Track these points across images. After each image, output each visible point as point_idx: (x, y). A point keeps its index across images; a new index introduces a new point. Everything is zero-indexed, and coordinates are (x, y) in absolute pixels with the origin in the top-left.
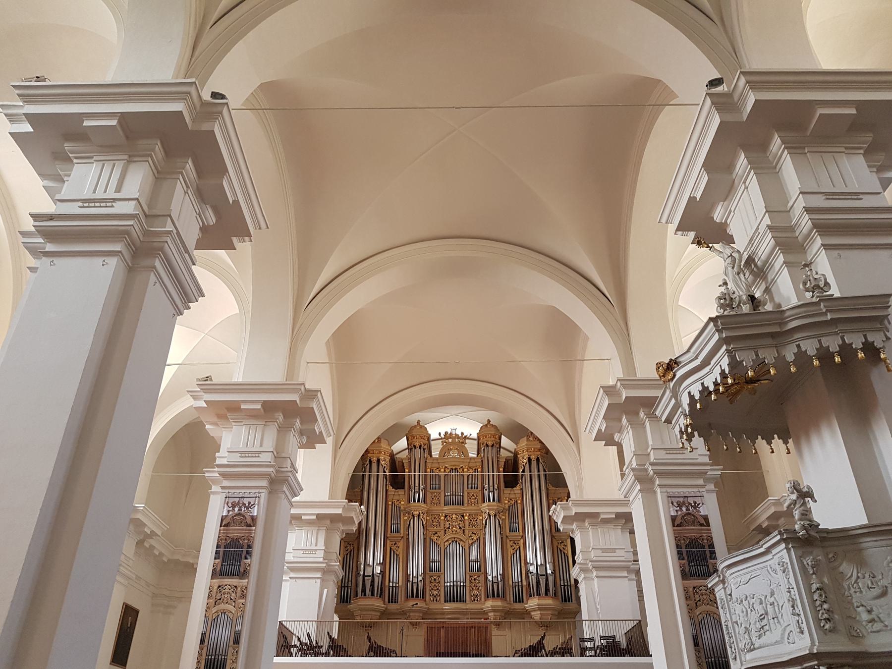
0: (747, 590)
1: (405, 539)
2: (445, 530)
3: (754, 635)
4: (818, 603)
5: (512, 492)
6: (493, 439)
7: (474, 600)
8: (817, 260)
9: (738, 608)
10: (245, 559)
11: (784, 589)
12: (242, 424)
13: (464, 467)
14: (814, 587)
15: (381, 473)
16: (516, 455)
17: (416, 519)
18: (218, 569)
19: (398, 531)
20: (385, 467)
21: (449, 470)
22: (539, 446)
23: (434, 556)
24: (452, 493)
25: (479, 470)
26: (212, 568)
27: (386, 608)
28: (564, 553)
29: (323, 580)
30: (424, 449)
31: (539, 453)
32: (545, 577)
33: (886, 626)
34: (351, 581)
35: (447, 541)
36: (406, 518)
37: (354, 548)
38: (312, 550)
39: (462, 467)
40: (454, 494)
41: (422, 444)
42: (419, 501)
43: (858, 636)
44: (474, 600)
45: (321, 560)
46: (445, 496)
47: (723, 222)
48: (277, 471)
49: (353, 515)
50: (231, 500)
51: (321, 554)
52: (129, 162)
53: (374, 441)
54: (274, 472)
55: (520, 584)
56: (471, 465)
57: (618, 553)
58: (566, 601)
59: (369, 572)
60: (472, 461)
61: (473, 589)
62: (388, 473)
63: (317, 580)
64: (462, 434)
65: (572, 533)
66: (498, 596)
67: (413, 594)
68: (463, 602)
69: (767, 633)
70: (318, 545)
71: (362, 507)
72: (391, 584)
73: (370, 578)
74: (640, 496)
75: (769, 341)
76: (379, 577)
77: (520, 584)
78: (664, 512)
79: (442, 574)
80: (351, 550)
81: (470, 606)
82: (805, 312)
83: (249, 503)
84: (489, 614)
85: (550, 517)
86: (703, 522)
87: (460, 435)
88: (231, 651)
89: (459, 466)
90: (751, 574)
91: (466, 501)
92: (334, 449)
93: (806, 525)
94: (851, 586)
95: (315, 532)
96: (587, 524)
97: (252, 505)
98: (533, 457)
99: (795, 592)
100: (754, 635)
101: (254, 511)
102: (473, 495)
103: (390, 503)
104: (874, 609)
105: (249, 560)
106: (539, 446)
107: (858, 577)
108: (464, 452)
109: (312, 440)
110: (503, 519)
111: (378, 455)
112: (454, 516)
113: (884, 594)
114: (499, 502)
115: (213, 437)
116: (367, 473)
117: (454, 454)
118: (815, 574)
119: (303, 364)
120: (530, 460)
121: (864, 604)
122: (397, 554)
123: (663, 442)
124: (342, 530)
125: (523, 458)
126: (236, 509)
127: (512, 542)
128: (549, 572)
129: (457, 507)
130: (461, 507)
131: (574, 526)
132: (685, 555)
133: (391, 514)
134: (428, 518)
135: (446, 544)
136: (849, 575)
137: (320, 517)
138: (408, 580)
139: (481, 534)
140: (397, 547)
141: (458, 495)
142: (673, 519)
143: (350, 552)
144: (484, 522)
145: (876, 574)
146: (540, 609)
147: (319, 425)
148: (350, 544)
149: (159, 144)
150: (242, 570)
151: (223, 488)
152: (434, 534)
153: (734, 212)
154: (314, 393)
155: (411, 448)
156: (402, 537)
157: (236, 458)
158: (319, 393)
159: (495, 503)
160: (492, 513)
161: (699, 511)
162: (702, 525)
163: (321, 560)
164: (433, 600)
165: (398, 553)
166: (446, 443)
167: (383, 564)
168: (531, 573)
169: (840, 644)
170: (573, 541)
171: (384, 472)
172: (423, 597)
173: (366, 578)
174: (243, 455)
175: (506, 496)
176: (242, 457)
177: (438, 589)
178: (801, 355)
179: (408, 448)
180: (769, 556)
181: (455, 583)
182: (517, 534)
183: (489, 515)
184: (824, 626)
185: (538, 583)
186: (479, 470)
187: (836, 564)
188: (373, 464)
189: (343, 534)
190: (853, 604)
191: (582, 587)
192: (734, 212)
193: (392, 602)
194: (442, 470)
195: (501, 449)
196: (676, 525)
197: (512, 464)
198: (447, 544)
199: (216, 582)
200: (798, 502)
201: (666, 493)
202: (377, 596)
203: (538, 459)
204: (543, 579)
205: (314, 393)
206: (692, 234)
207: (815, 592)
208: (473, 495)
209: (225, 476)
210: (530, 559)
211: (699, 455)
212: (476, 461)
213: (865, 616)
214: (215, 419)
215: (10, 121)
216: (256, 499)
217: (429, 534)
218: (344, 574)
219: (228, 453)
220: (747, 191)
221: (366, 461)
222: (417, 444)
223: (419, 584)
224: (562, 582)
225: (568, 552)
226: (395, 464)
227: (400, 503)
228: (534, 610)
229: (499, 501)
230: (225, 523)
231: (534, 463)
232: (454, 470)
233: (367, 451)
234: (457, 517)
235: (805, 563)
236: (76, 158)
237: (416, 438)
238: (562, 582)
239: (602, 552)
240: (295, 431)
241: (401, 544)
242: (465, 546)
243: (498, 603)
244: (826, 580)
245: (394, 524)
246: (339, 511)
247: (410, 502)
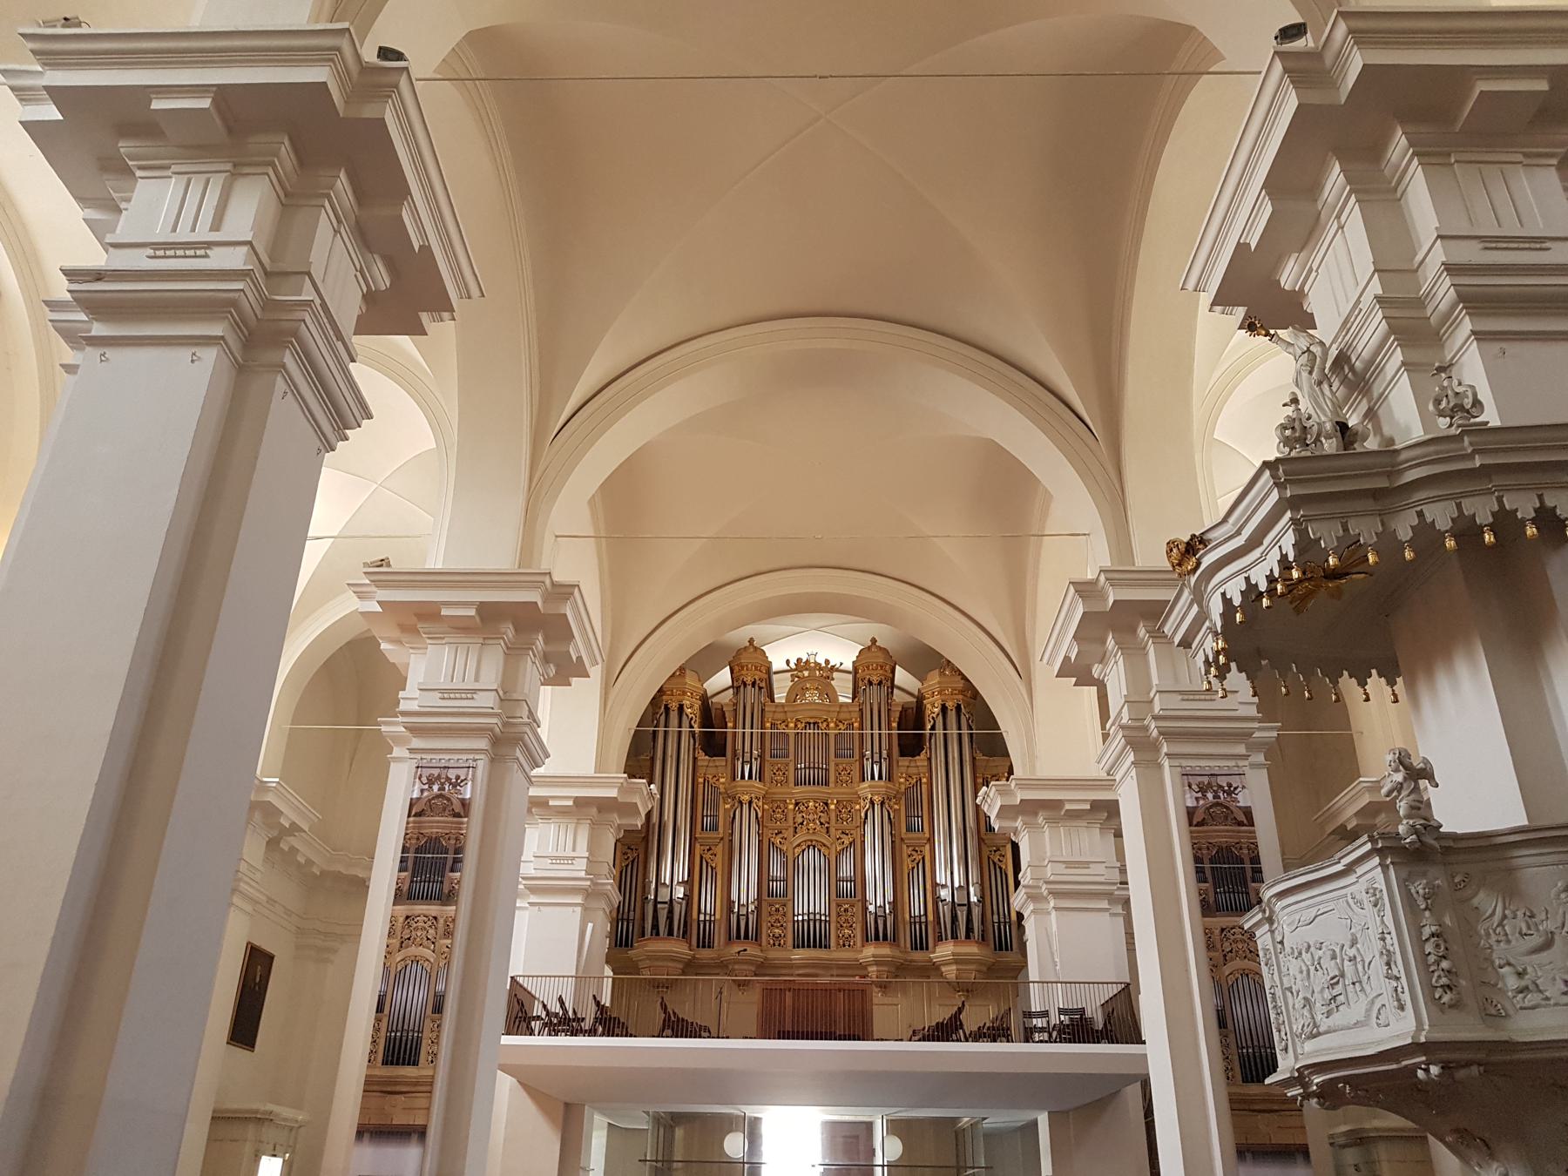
0: (1310, 935)
1: (726, 840)
2: (796, 828)
3: (1319, 1009)
4: (1432, 959)
5: (913, 764)
6: (881, 672)
7: (844, 945)
8: (1463, 358)
9: (1293, 966)
10: (452, 870)
11: (1374, 933)
12: (444, 642)
13: (829, 720)
14: (1427, 932)
15: (685, 729)
16: (920, 699)
17: (746, 807)
18: (405, 888)
19: (715, 828)
20: (692, 719)
21: (803, 725)
22: (961, 684)
23: (776, 871)
24: (807, 764)
25: (856, 725)
26: (394, 887)
27: (694, 957)
28: (1000, 868)
29: (585, 909)
30: (760, 688)
31: (961, 697)
32: (965, 908)
33: (1547, 999)
34: (634, 911)
35: (799, 845)
36: (727, 806)
37: (638, 856)
38: (567, 858)
39: (826, 720)
40: (812, 765)
41: (757, 679)
42: (750, 777)
43: (1499, 1016)
44: (844, 945)
45: (583, 874)
46: (796, 769)
47: (1297, 289)
48: (505, 724)
49: (637, 800)
50: (426, 772)
51: (582, 864)
52: (235, 175)
53: (674, 673)
55: (923, 919)
56: (842, 716)
57: (1094, 869)
58: (1001, 949)
59: (664, 895)
60: (845, 709)
61: (841, 926)
62: (697, 729)
64: (827, 662)
65: (1015, 834)
66: (885, 938)
67: (740, 934)
68: (825, 947)
69: (1341, 1008)
70: (578, 848)
71: (652, 786)
72: (702, 917)
73: (666, 906)
74: (1133, 773)
75: (1369, 504)
76: (681, 904)
77: (923, 919)
78: (1175, 800)
79: (789, 900)
80: (634, 859)
81: (835, 954)
82: (1437, 453)
83: (458, 777)
84: (870, 969)
85: (977, 807)
86: (1242, 818)
87: (824, 665)
88: (428, 1024)
89: (820, 718)
90: (1317, 908)
91: (832, 779)
92: (604, 686)
93: (1418, 826)
94: (1491, 931)
95: (571, 827)
96: (1040, 819)
97: (462, 781)
98: (950, 705)
99: (1392, 940)
100: (1319, 1009)
101: (465, 791)
102: (845, 769)
103: (701, 780)
104: (1529, 970)
105: (459, 874)
106: (961, 684)
107: (1504, 917)
108: (830, 694)
109: (564, 670)
110: (895, 810)
111: (681, 698)
112: (811, 804)
113: (1548, 944)
114: (889, 780)
115: (394, 664)
116: (662, 729)
117: (812, 697)
118: (1430, 910)
119: (549, 539)
120: (944, 709)
121: (1512, 961)
122: (712, 867)
123: (1176, 680)
124: (619, 825)
125: (933, 706)
126: (436, 787)
127: (910, 849)
128: (974, 899)
129: (816, 788)
130: (824, 789)
131: (1019, 823)
132: (1208, 874)
133: (702, 800)
134: (766, 806)
135: (796, 850)
136: (1490, 911)
137: (580, 803)
138: (730, 910)
139: (857, 834)
140: (712, 855)
141: (818, 768)
142: (1191, 813)
143: (633, 862)
144: (863, 815)
145: (1535, 911)
146: (956, 962)
147: (576, 646)
148: (632, 850)
149: (287, 142)
150: (446, 891)
151: (411, 750)
152: (776, 834)
153: (1317, 271)
154: (569, 590)
155: (738, 685)
156: (722, 839)
157: (434, 700)
158: (576, 590)
159: (882, 783)
160: (877, 799)
161: (1236, 800)
162: (1240, 824)
163: (583, 874)
164: (774, 945)
165: (714, 865)
166: (798, 677)
167: (688, 883)
168: (942, 901)
169: (1467, 1029)
170: (1015, 848)
171: (691, 727)
172: (757, 938)
173: (659, 906)
174: (446, 695)
175: (903, 769)
176: (444, 699)
177: (782, 926)
178: (1426, 534)
179: (732, 687)
180: (1351, 879)
181: (812, 917)
182: (920, 835)
183: (872, 803)
184: (1440, 997)
185: (954, 918)
186: (856, 725)
187: (1469, 892)
188: (671, 712)
189: (620, 831)
190: (1492, 962)
191: (1029, 924)
192: (1317, 271)
193: (704, 947)
194: (792, 725)
195: (895, 691)
196: (1195, 823)
197: (913, 716)
198: (798, 850)
199: (402, 910)
200: (1405, 785)
201: (1179, 769)
202: (678, 936)
203: (958, 708)
204: (962, 912)
205: (569, 590)
206: (1240, 312)
207: (1427, 940)
208: (845, 769)
209: (416, 730)
210: (941, 878)
211: (1241, 703)
212: (851, 709)
213: (1512, 983)
214: (396, 633)
215: (21, 100)
216: (468, 771)
217: (768, 833)
218: (622, 899)
219: (419, 691)
220: (1343, 232)
221: (659, 708)
222: (749, 680)
223: (750, 916)
224: (996, 917)
225: (1006, 867)
226: (709, 713)
227: (718, 780)
228: (947, 964)
229: (890, 779)
230: (416, 810)
231: (952, 715)
232: (812, 725)
233: (661, 691)
234: (817, 805)
235: (1413, 891)
236: (141, 168)
237: (747, 670)
238: (996, 917)
240: (535, 656)
241: (719, 849)
242: (829, 855)
243: (885, 950)
244: (1447, 921)
245: (707, 816)
246: (613, 793)
247: (734, 780)
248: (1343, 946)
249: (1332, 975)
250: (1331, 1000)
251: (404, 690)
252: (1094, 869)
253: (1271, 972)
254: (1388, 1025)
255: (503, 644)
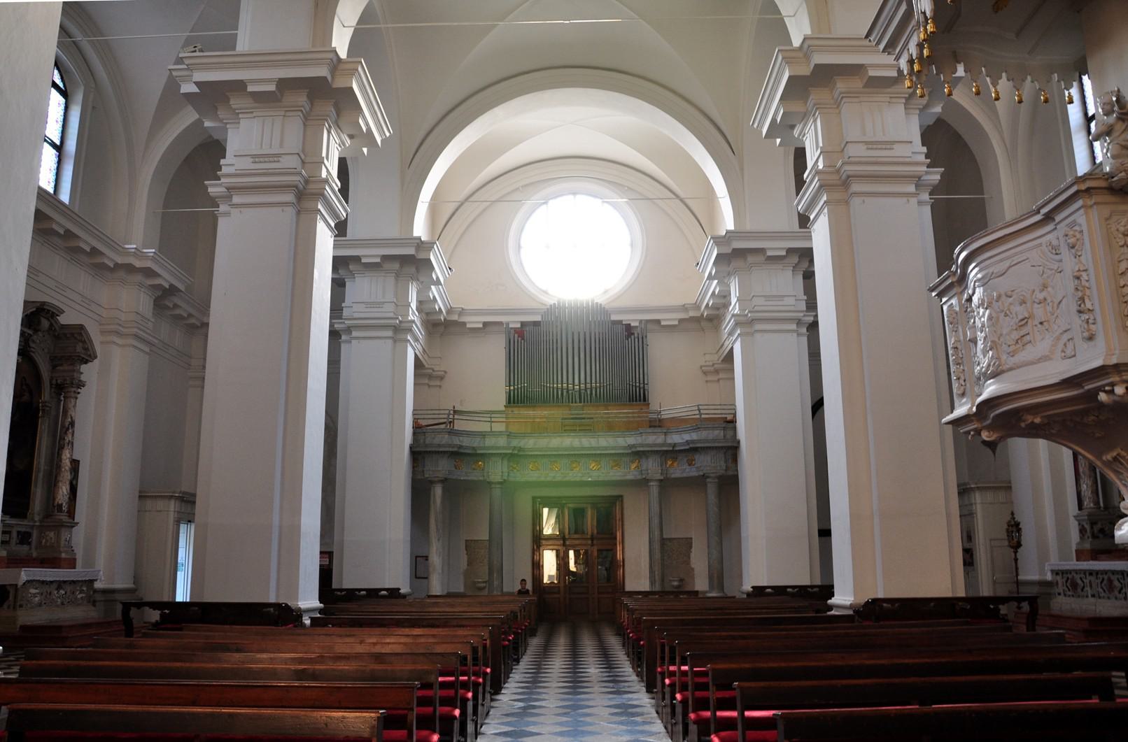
54: (302, 182)
63: (285, 209)
176: (256, 162)
239: (868, 149)
248: (1034, 291)
249: (1020, 317)
250: (1018, 339)
251: (225, 158)
252: (900, 151)
253: (955, 329)
254: (1074, 356)
255: (301, 115)
